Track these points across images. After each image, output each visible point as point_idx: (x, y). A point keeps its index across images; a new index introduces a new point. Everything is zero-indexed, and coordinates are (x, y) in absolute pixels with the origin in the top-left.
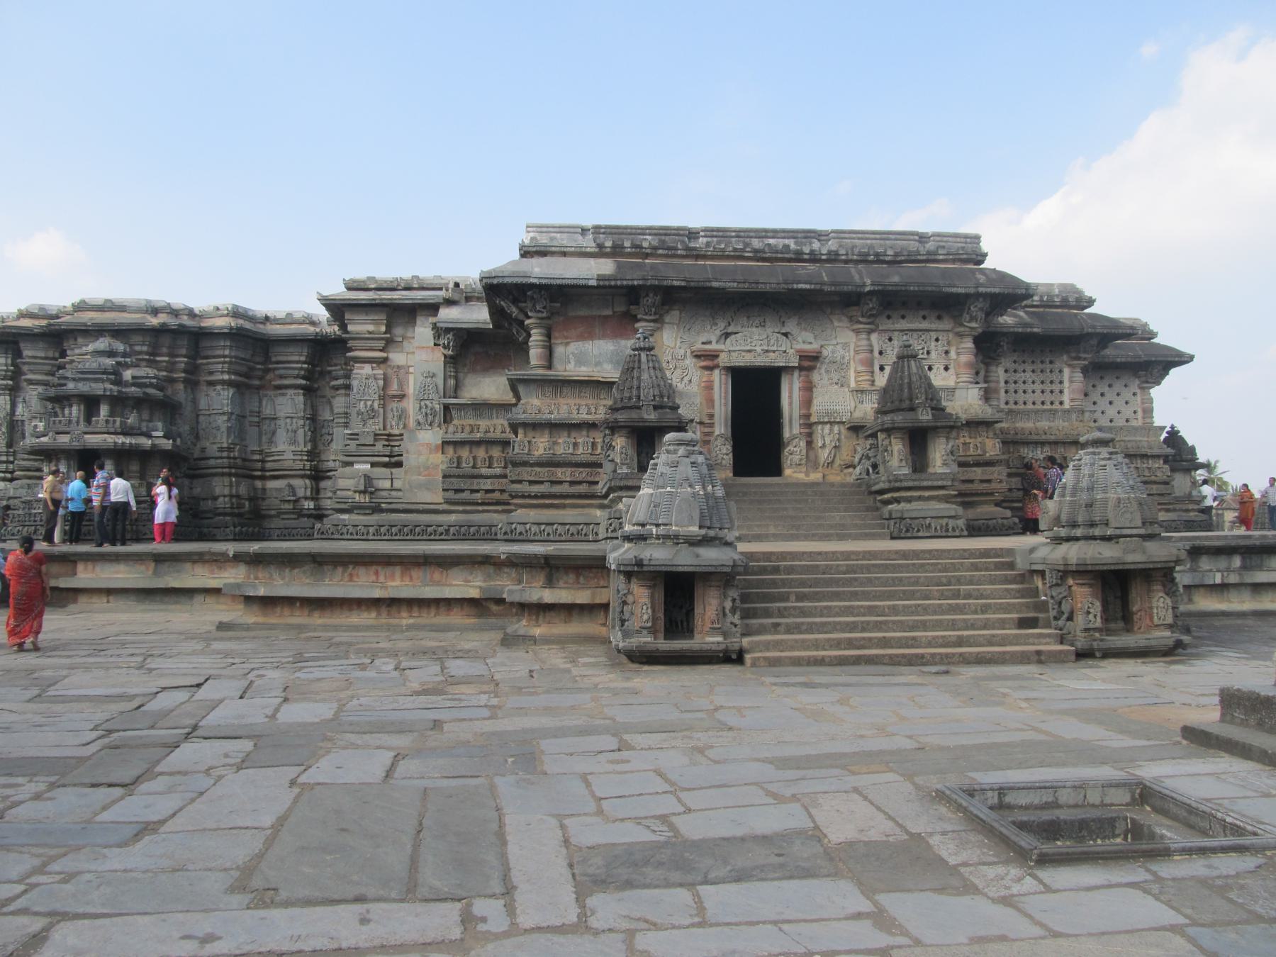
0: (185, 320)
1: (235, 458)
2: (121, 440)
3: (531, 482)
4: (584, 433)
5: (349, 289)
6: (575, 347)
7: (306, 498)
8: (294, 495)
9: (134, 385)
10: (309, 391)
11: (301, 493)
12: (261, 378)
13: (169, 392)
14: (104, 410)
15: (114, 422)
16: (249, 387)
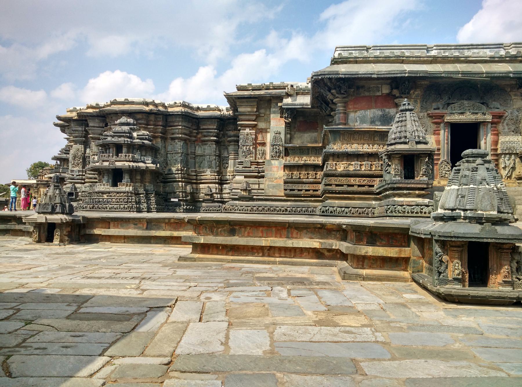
0: (161, 108)
1: (184, 174)
2: (131, 164)
3: (337, 185)
4: (366, 159)
5: (238, 90)
6: (359, 113)
7: (216, 193)
8: (211, 191)
9: (138, 138)
10: (217, 142)
11: (214, 191)
12: (195, 137)
13: (154, 143)
14: (124, 150)
15: (129, 156)
16: (190, 141)
